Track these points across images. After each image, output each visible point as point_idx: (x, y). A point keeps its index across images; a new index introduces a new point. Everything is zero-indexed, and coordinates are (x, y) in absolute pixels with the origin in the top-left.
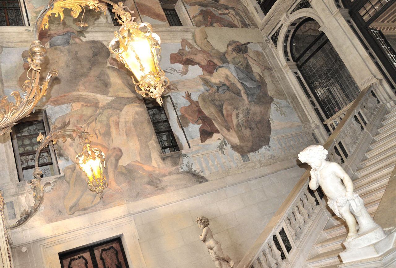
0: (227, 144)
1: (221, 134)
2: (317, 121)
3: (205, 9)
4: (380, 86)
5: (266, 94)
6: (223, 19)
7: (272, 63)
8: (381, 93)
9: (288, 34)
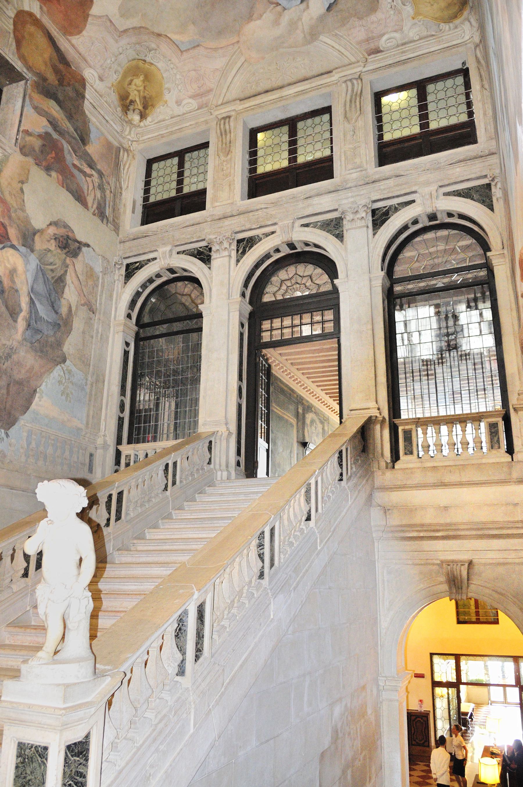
2: (111, 439)
3: (55, 136)
4: (225, 441)
5: (59, 344)
6: (73, 176)
7: (103, 302)
8: (220, 451)
9: (154, 278)
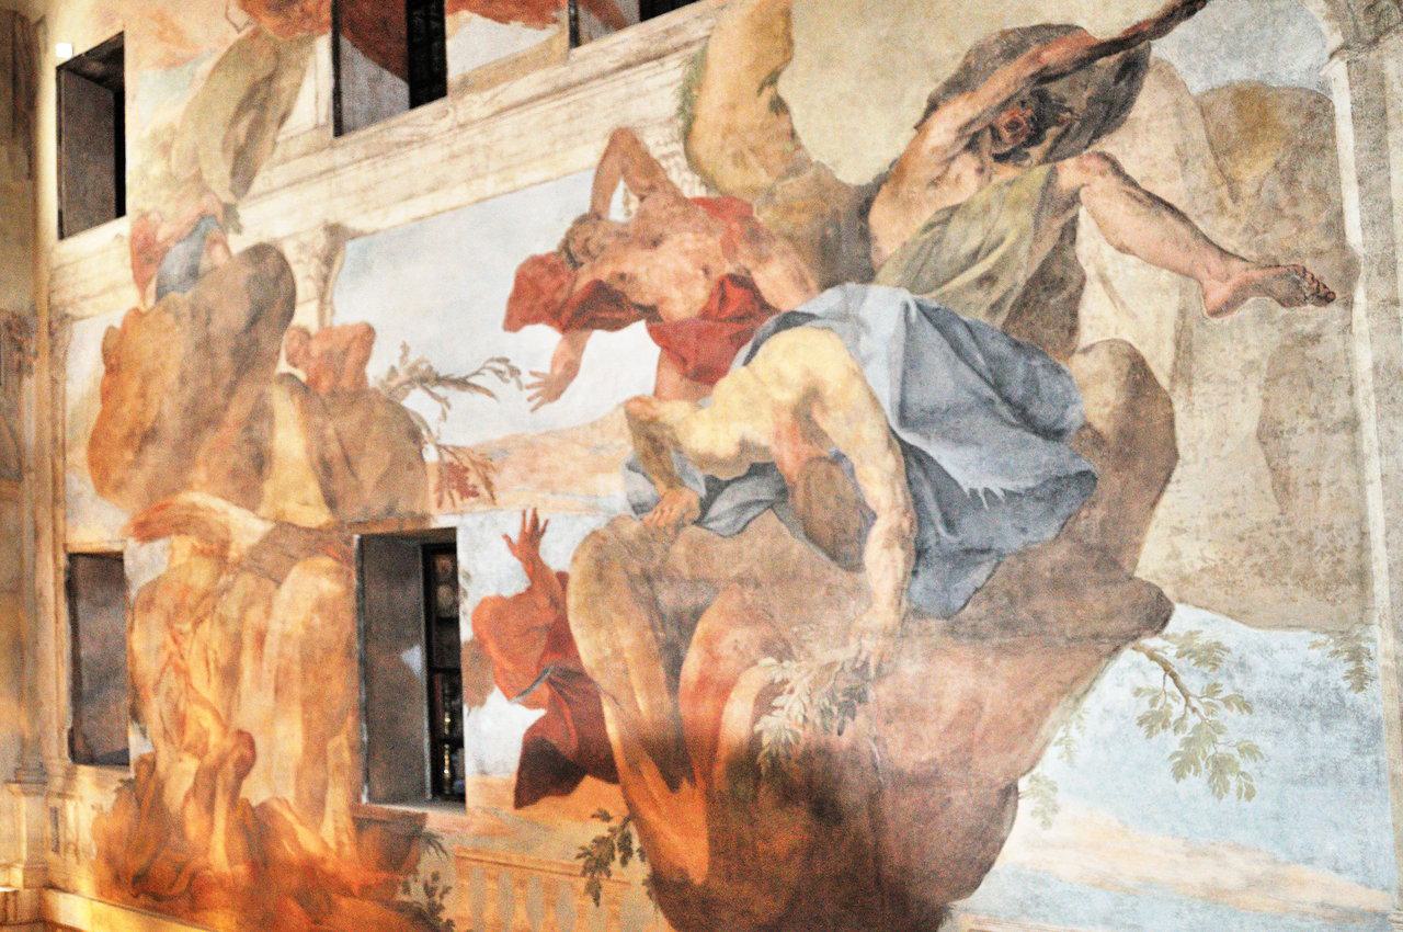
0: (636, 855)
1: (624, 789)
